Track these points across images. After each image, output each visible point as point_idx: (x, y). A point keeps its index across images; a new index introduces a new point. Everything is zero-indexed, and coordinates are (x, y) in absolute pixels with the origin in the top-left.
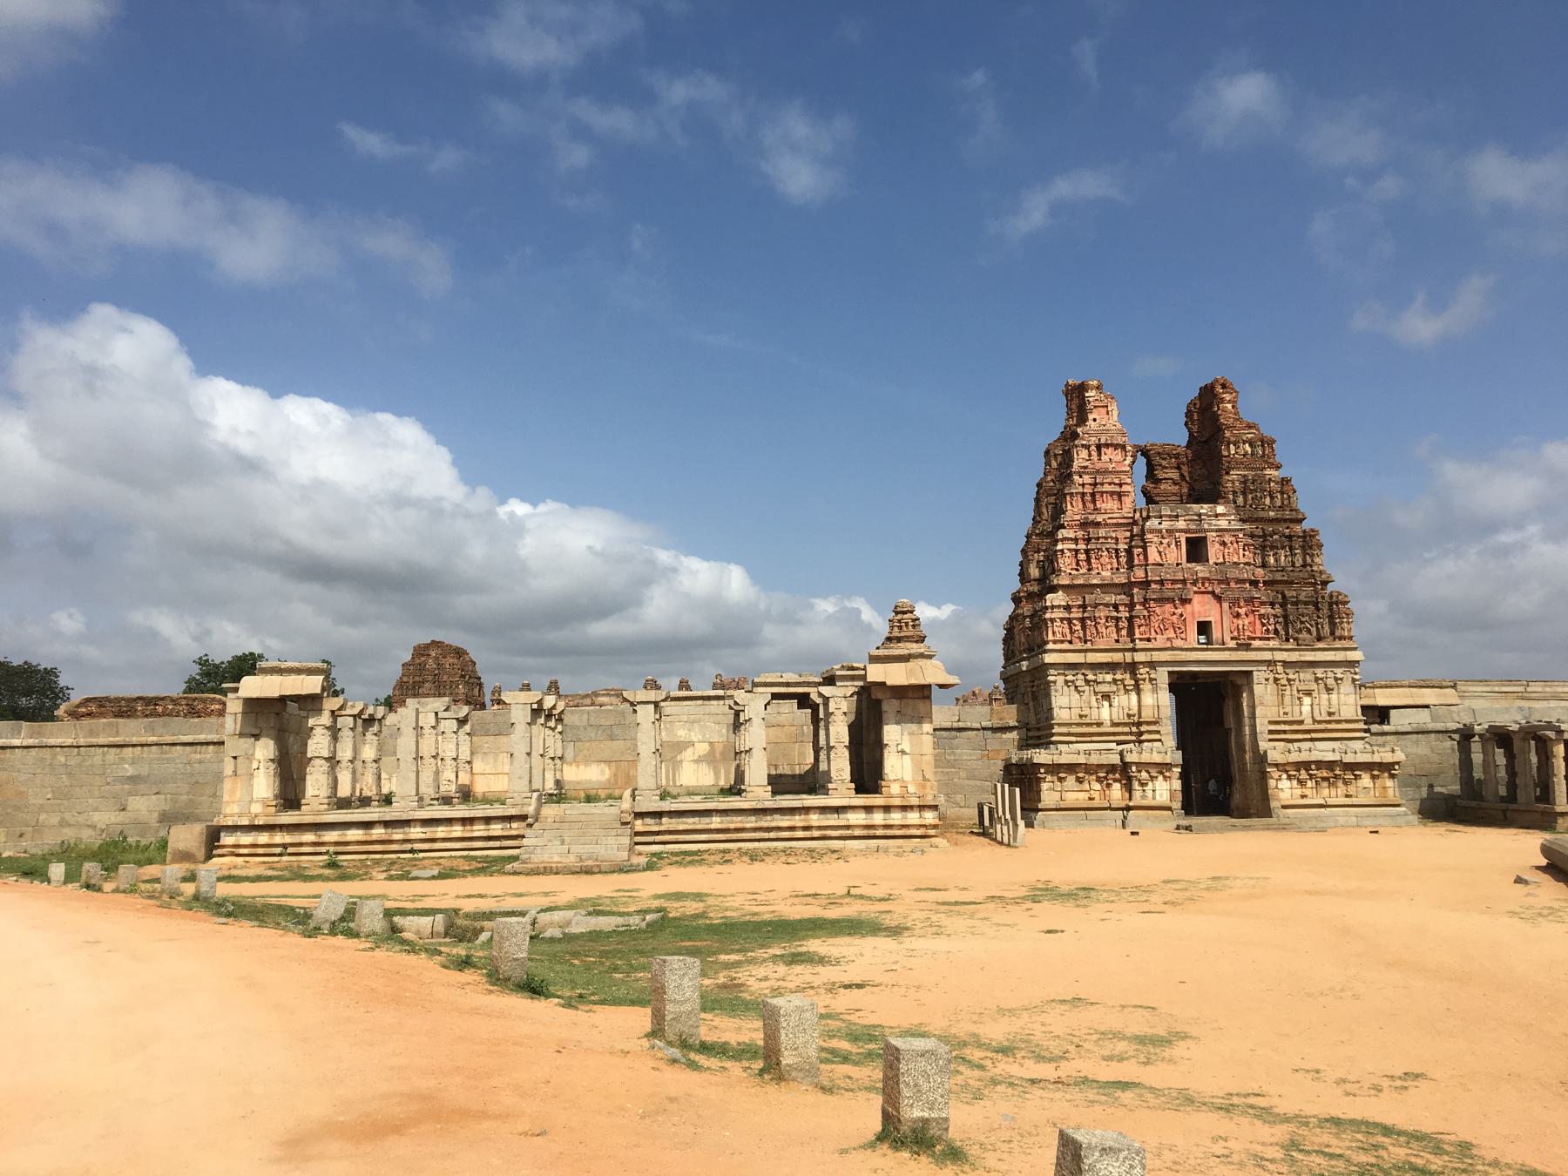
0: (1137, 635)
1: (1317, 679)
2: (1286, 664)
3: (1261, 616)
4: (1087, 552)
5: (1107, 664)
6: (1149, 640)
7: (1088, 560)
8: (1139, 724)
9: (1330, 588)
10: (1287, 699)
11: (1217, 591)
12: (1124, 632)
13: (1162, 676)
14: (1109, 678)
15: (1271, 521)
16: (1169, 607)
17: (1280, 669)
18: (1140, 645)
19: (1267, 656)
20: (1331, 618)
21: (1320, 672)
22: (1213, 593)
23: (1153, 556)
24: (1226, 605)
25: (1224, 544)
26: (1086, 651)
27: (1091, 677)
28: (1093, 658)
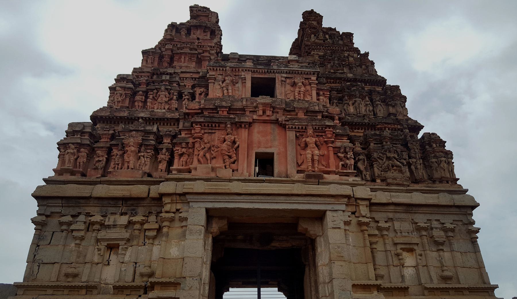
0: (175, 166)
1: (419, 229)
2: (372, 205)
3: (337, 150)
4: (146, 94)
5: (125, 200)
6: (190, 172)
7: (145, 102)
8: (152, 286)
9: (420, 136)
10: (380, 258)
11: (282, 118)
12: (163, 166)
13: (197, 215)
14: (123, 220)
15: (348, 80)
16: (218, 135)
17: (364, 210)
18: (175, 175)
19: (347, 190)
20: (425, 158)
21: (421, 219)
22: (276, 122)
23: (215, 91)
24: (291, 135)
25: (294, 85)
26: (100, 183)
27: (97, 218)
28: (101, 190)
